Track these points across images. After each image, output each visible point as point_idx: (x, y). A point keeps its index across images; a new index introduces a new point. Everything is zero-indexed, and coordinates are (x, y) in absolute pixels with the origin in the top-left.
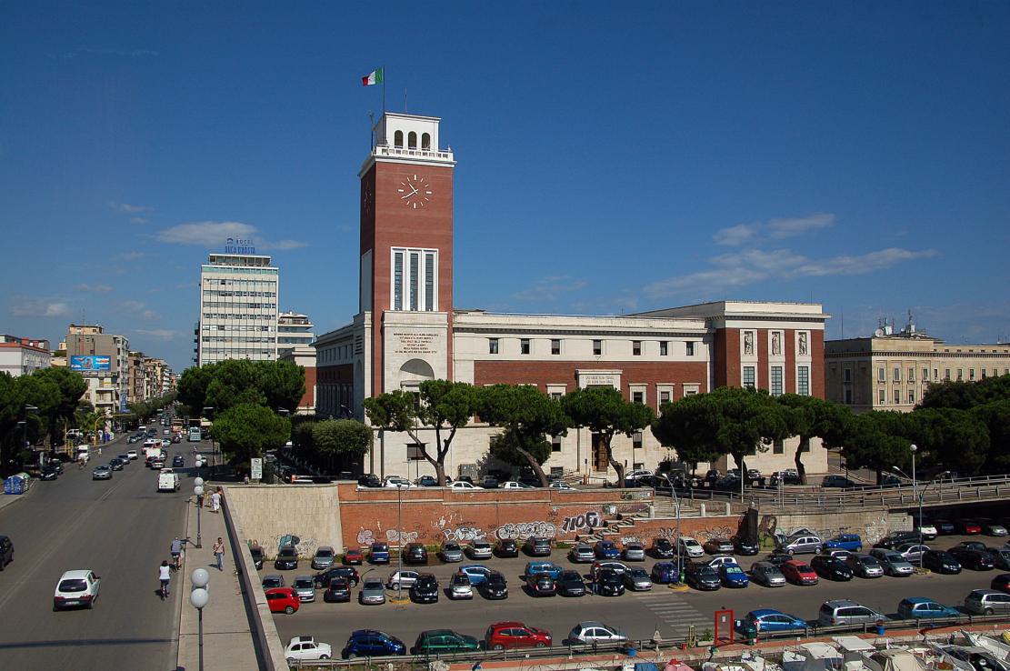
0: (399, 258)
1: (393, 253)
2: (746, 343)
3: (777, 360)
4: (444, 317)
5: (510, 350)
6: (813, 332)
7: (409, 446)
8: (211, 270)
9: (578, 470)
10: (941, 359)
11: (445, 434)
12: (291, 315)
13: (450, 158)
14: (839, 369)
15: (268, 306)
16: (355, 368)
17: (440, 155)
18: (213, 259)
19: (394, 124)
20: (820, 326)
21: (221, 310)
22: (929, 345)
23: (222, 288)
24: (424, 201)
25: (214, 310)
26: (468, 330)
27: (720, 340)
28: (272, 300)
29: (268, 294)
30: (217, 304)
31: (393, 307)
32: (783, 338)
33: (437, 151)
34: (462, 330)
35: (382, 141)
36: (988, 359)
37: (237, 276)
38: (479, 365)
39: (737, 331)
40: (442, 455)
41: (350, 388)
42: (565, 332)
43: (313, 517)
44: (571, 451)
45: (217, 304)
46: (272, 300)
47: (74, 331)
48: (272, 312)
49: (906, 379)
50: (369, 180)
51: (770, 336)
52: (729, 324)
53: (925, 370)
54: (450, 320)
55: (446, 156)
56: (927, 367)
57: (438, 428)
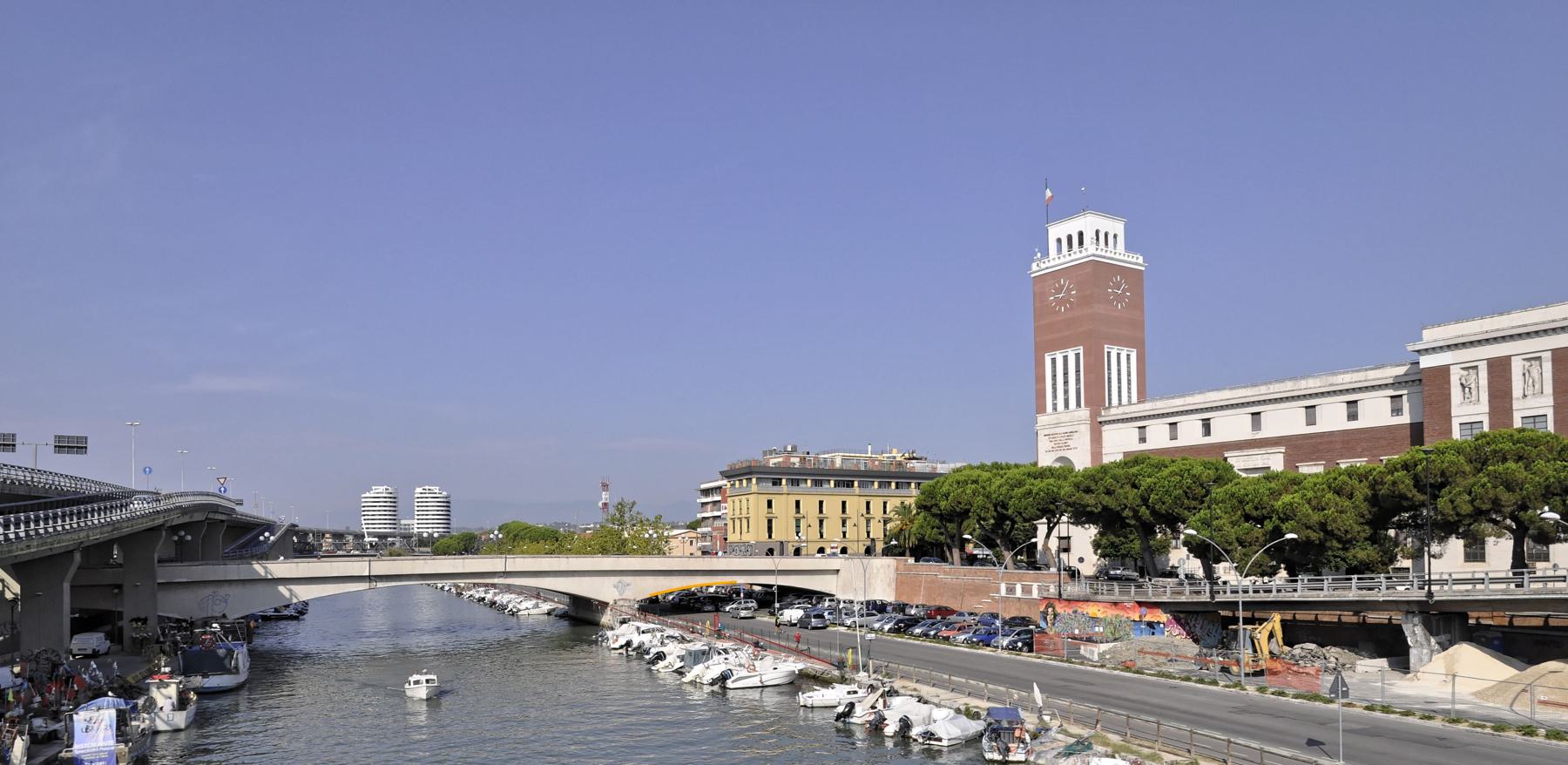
0: (1054, 361)
4: (1084, 413)
5: (1159, 437)
31: (1049, 408)
32: (1548, 367)
34: (1110, 422)
38: (1125, 454)
39: (1444, 371)
42: (1265, 402)
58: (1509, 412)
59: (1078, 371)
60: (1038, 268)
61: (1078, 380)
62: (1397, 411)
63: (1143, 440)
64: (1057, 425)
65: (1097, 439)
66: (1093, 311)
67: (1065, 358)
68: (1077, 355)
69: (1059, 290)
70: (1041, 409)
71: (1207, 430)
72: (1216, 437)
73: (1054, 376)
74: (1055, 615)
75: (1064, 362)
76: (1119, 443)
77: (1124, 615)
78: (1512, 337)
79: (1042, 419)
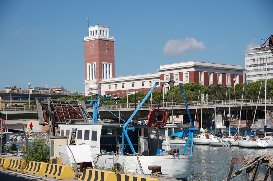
5: (113, 88)
6: (190, 72)
21: (253, 73)
23: (253, 63)
25: (251, 74)
30: (252, 71)
32: (179, 76)
35: (87, 35)
37: (259, 57)
38: (106, 92)
45: (252, 71)
60: (86, 39)
65: (99, 88)
66: (105, 51)
70: (86, 79)
73: (89, 70)
75: (92, 66)
76: (104, 89)
79: (86, 82)
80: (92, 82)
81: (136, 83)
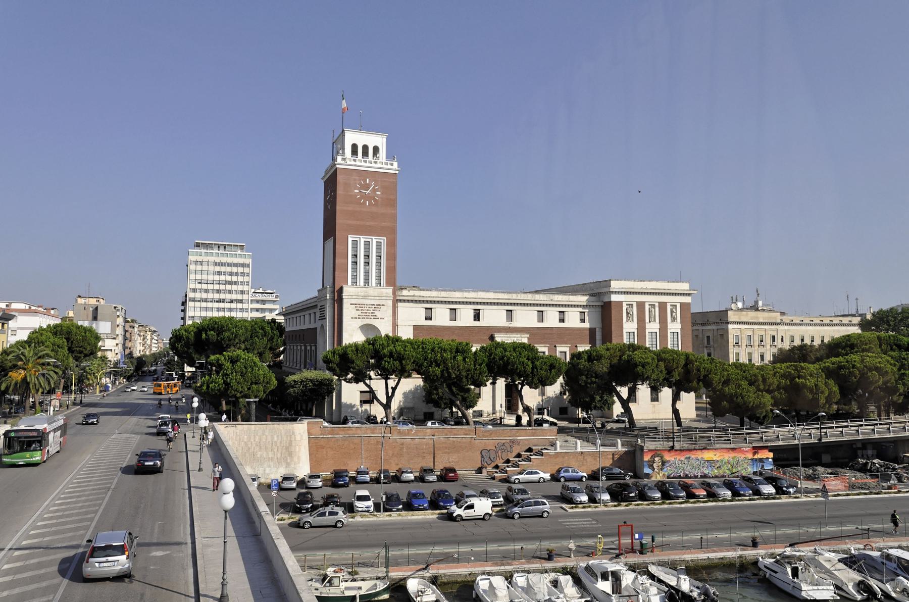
0: (355, 243)
1: (350, 240)
2: (628, 313)
3: (653, 327)
4: (390, 290)
5: (442, 317)
7: (361, 392)
8: (197, 254)
9: (494, 413)
10: (786, 327)
11: (392, 383)
12: (261, 291)
13: (396, 164)
14: (701, 336)
15: (242, 283)
16: (318, 330)
17: (387, 164)
18: (198, 245)
19: (352, 137)
20: (688, 300)
22: (777, 317)
24: (375, 201)
26: (408, 301)
27: (605, 312)
28: (246, 279)
29: (243, 274)
32: (657, 309)
33: (384, 160)
34: (404, 301)
36: (826, 328)
38: (416, 328)
39: (620, 303)
40: (389, 399)
41: (313, 348)
43: (287, 448)
44: (491, 398)
46: (246, 279)
47: (81, 301)
48: (246, 288)
49: (757, 343)
50: (331, 181)
51: (647, 307)
52: (614, 298)
53: (774, 338)
54: (394, 293)
55: (392, 165)
56: (774, 334)
57: (386, 379)
58: (645, 328)
59: (379, 257)
61: (379, 264)
62: (583, 321)
63: (429, 318)
64: (365, 297)
67: (367, 244)
68: (379, 245)
69: (367, 187)
71: (477, 317)
72: (484, 322)
74: (663, 463)
77: (741, 456)
78: (681, 294)
80: (370, 291)
81: (518, 312)
